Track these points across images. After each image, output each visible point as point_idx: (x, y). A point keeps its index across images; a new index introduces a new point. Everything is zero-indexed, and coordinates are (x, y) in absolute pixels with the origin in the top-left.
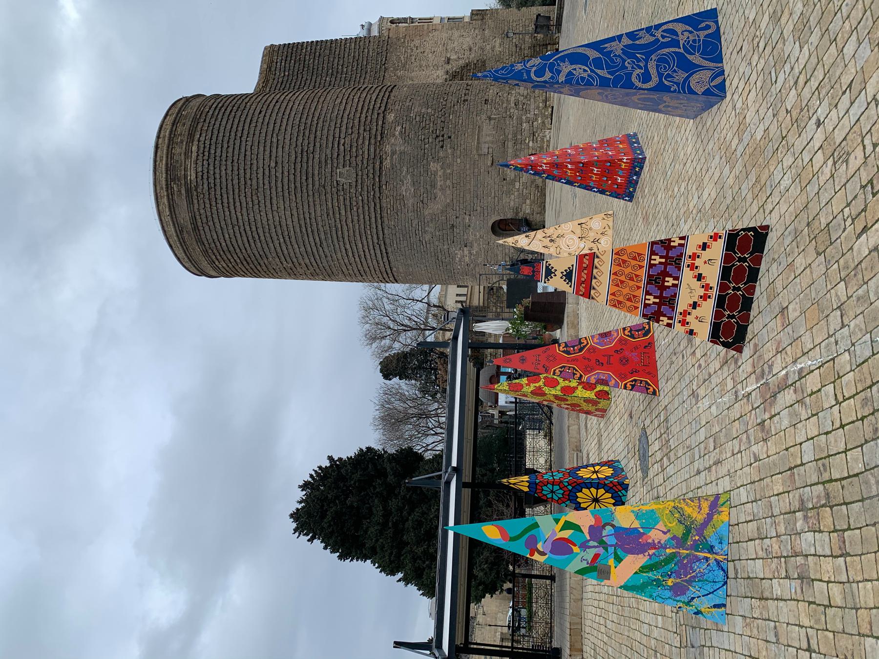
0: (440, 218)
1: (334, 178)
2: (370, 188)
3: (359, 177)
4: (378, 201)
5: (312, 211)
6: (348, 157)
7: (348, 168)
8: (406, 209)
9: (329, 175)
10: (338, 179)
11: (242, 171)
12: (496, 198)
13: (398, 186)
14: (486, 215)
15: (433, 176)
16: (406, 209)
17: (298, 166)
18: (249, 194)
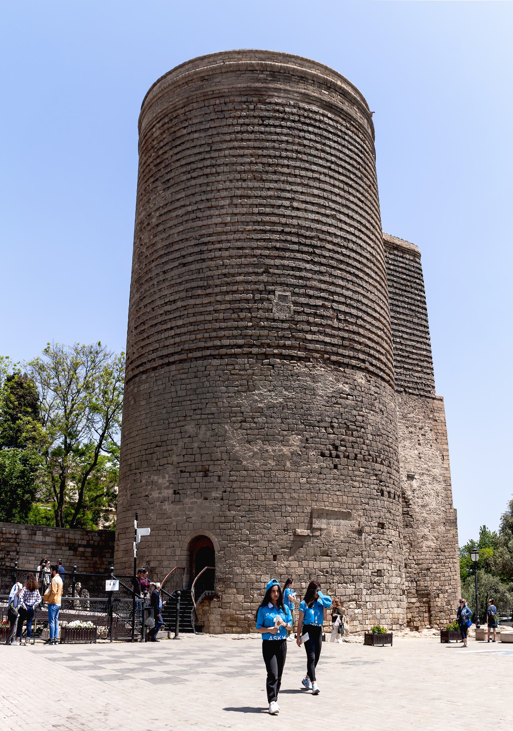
3: (279, 325)
6: (308, 310)
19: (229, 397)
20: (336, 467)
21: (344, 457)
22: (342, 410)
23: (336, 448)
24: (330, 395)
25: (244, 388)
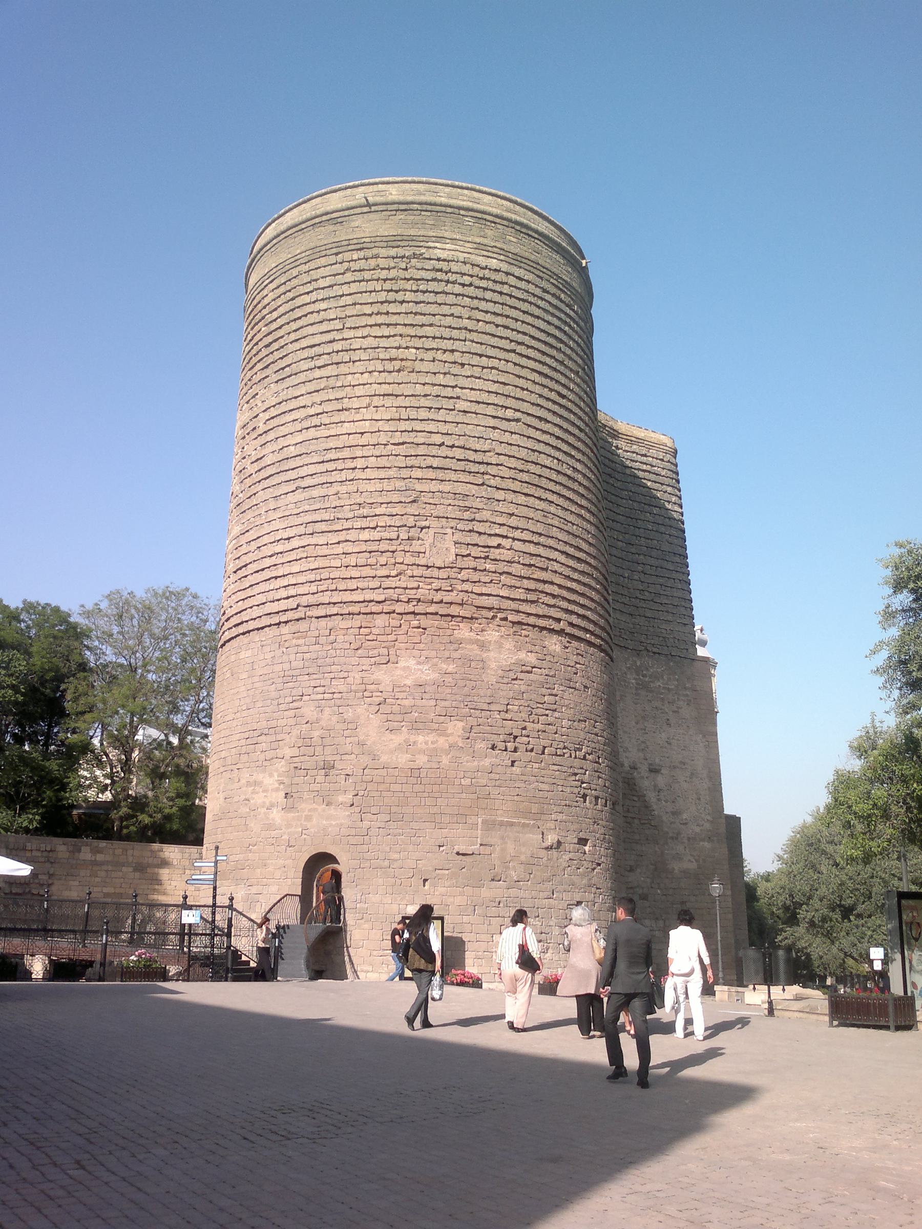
3: (436, 573)
4: (387, 608)
5: (369, 473)
10: (431, 531)
11: (448, 345)
17: (459, 454)
18: (401, 353)
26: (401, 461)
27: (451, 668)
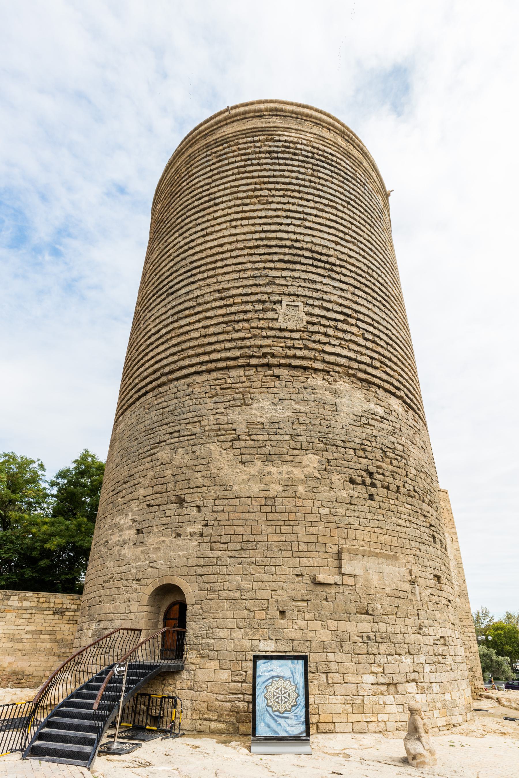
0: (199, 475)
1: (286, 298)
2: (266, 350)
3: (287, 334)
4: (241, 362)
6: (324, 322)
7: (306, 318)
8: (223, 410)
9: (291, 290)
10: (284, 304)
11: (297, 188)
12: (237, 594)
13: (271, 396)
14: (200, 570)
15: (291, 458)
16: (223, 410)
19: (217, 413)
20: (371, 497)
21: (383, 487)
22: (376, 433)
23: (371, 474)
24: (360, 414)
25: (238, 403)
26: (256, 258)
27: (304, 408)
